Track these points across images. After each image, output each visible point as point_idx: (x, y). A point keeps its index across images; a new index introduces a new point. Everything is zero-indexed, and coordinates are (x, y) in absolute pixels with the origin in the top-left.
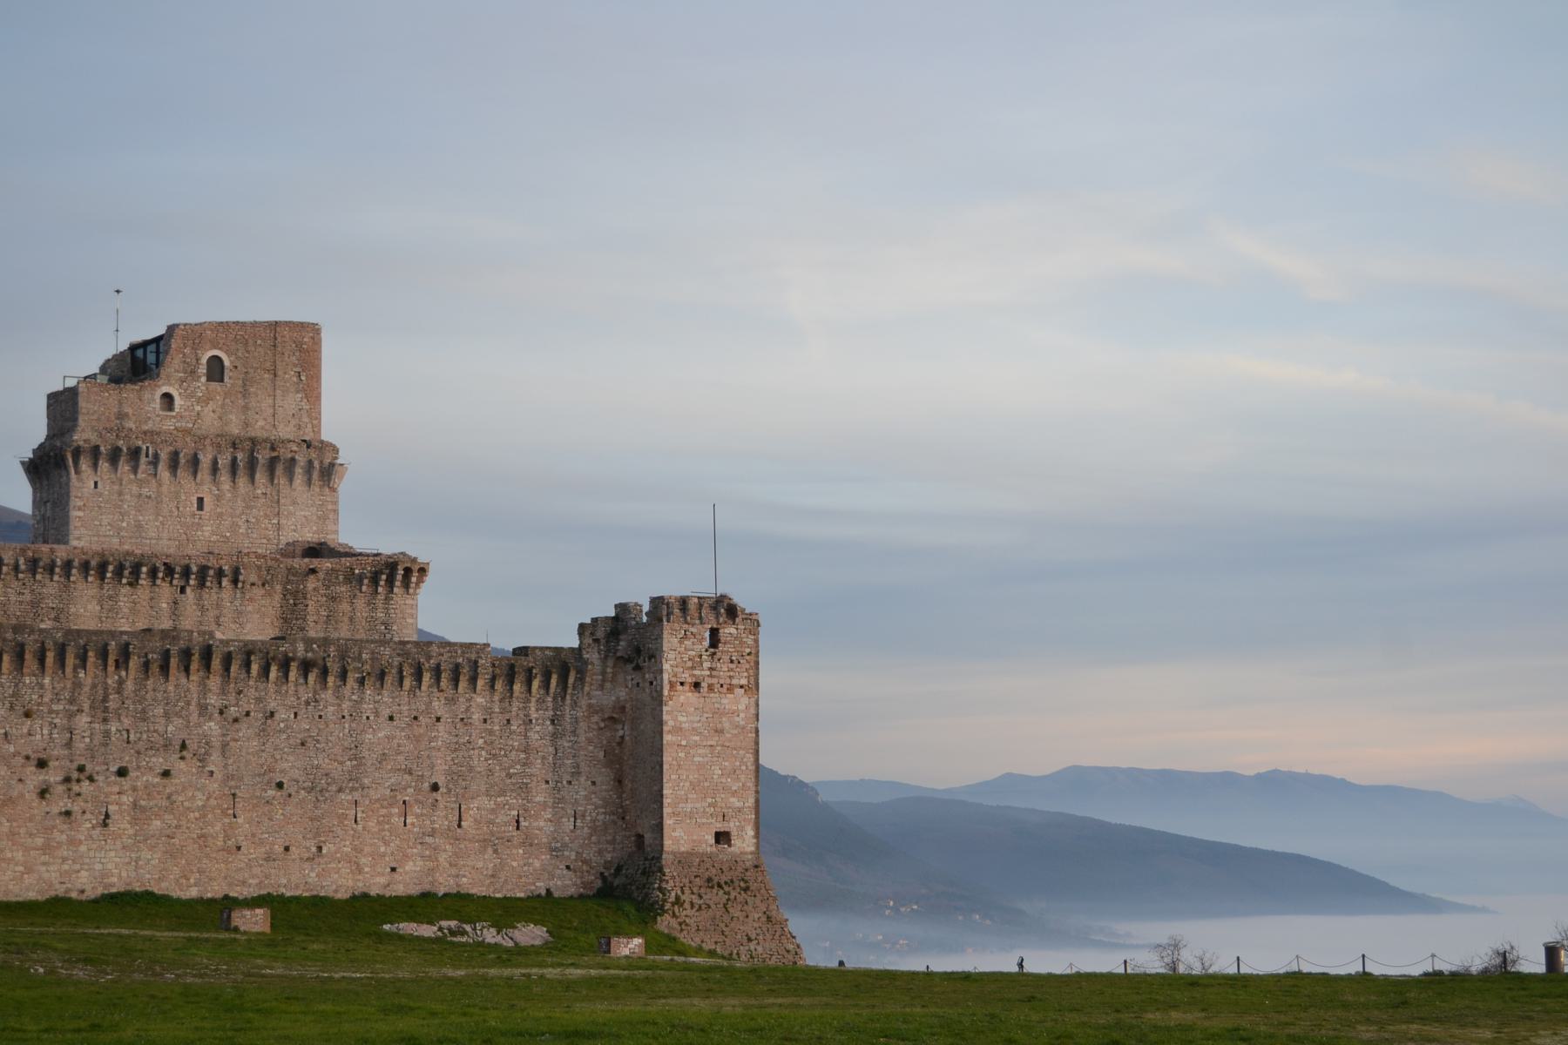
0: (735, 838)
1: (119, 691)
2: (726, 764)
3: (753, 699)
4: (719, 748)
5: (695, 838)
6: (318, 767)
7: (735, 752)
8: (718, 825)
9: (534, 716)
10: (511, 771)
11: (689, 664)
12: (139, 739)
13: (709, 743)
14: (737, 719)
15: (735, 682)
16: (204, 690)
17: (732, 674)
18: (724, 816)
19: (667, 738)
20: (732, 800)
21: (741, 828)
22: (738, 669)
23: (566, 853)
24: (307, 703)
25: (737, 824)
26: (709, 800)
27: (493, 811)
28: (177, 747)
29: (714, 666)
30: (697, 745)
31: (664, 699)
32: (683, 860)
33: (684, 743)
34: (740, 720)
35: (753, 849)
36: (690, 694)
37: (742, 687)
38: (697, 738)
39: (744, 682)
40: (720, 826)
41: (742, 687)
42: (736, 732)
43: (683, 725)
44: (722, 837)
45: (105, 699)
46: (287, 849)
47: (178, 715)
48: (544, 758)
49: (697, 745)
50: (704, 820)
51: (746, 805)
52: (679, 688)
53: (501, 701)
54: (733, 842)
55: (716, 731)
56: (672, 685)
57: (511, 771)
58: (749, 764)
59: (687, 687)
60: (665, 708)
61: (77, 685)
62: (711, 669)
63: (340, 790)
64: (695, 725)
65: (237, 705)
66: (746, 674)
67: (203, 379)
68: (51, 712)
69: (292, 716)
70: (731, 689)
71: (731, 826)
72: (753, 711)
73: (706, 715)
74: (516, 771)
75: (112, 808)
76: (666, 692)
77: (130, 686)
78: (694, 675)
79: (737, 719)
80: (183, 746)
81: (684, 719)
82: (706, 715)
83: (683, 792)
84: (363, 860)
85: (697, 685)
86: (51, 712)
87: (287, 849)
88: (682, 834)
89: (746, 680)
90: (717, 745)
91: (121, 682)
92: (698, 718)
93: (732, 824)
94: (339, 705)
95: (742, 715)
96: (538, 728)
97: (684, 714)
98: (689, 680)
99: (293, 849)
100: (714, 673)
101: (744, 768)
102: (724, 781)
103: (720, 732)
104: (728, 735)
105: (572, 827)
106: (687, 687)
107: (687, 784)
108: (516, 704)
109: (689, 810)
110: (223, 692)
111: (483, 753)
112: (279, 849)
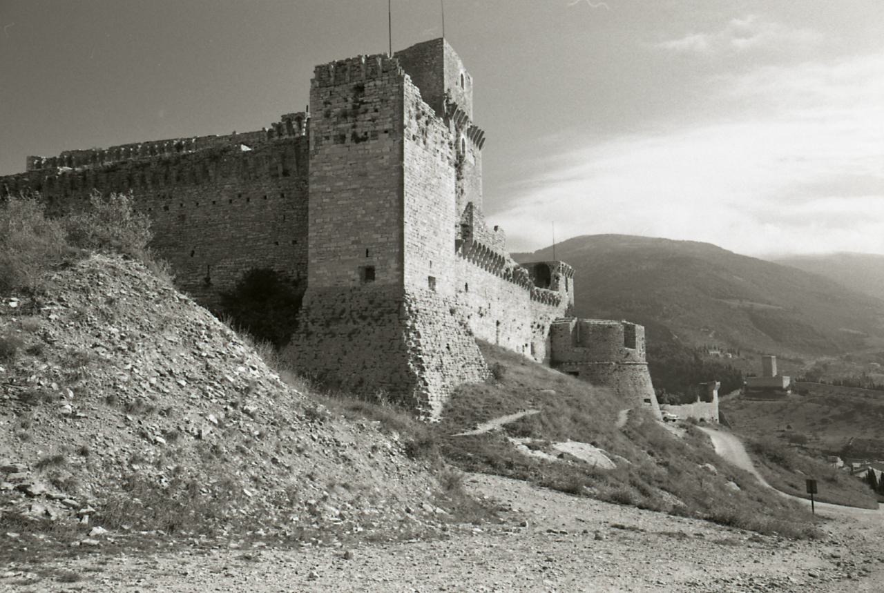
0: (378, 271)
2: (370, 203)
3: (398, 141)
4: (362, 190)
5: (338, 274)
7: (378, 192)
8: (362, 261)
10: (248, 237)
13: (354, 186)
14: (381, 161)
18: (367, 252)
19: (313, 187)
20: (375, 236)
21: (385, 262)
22: (382, 117)
25: (381, 258)
26: (353, 238)
30: (341, 190)
31: (311, 153)
32: (322, 294)
33: (328, 189)
34: (384, 162)
35: (397, 280)
36: (335, 146)
37: (386, 132)
38: (341, 183)
39: (387, 127)
40: (366, 262)
42: (379, 173)
43: (328, 174)
44: (369, 273)
49: (341, 190)
50: (348, 257)
51: (390, 239)
52: (324, 142)
54: (376, 275)
55: (360, 175)
56: (318, 141)
57: (248, 237)
58: (393, 201)
60: (311, 162)
64: (339, 172)
66: (390, 119)
70: (375, 135)
71: (375, 260)
72: (397, 152)
73: (349, 162)
74: (252, 237)
76: (312, 148)
78: (338, 129)
79: (381, 161)
81: (326, 168)
82: (349, 162)
83: (326, 234)
85: (343, 138)
88: (326, 271)
89: (391, 125)
90: (361, 188)
92: (343, 166)
93: (375, 259)
95: (386, 157)
97: (329, 164)
98: (334, 133)
101: (388, 205)
102: (367, 219)
103: (363, 175)
104: (372, 177)
107: (331, 226)
109: (333, 249)
111: (228, 226)
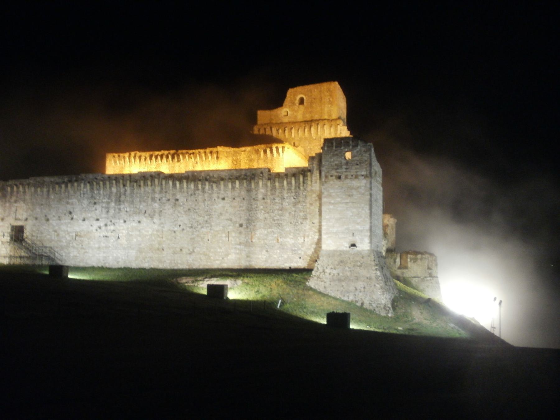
1: (125, 194)
6: (194, 219)
9: (286, 195)
11: (336, 167)
12: (131, 211)
15: (359, 173)
16: (154, 191)
17: (357, 170)
23: (299, 252)
24: (191, 195)
25: (360, 237)
27: (267, 235)
28: (143, 213)
29: (348, 167)
37: (363, 176)
39: (363, 173)
41: (363, 176)
45: (120, 197)
46: (181, 250)
47: (144, 201)
48: (290, 213)
53: (271, 190)
59: (334, 177)
61: (111, 192)
62: (346, 169)
63: (202, 227)
65: (165, 197)
67: (297, 105)
68: (102, 202)
69: (185, 200)
75: (120, 235)
77: (128, 192)
80: (145, 212)
84: (211, 254)
86: (102, 202)
87: (181, 250)
91: (126, 191)
93: (357, 238)
94: (203, 195)
96: (287, 200)
99: (183, 250)
100: (347, 170)
105: (303, 241)
106: (334, 177)
108: (277, 191)
110: (161, 192)
112: (178, 250)
